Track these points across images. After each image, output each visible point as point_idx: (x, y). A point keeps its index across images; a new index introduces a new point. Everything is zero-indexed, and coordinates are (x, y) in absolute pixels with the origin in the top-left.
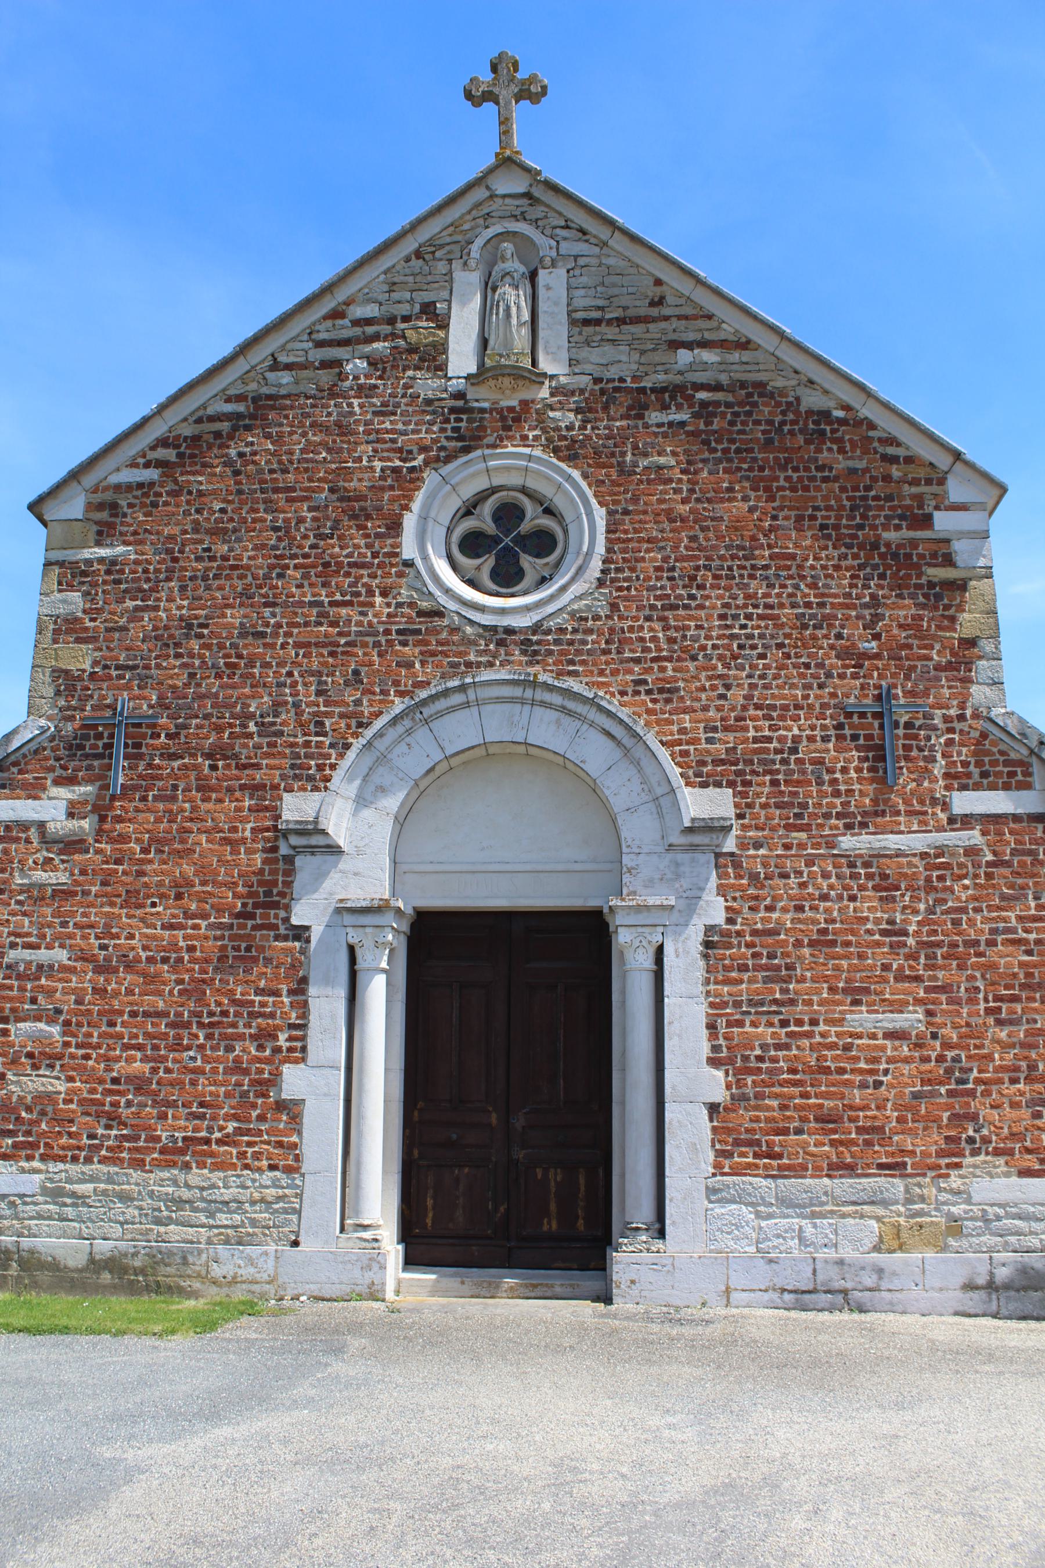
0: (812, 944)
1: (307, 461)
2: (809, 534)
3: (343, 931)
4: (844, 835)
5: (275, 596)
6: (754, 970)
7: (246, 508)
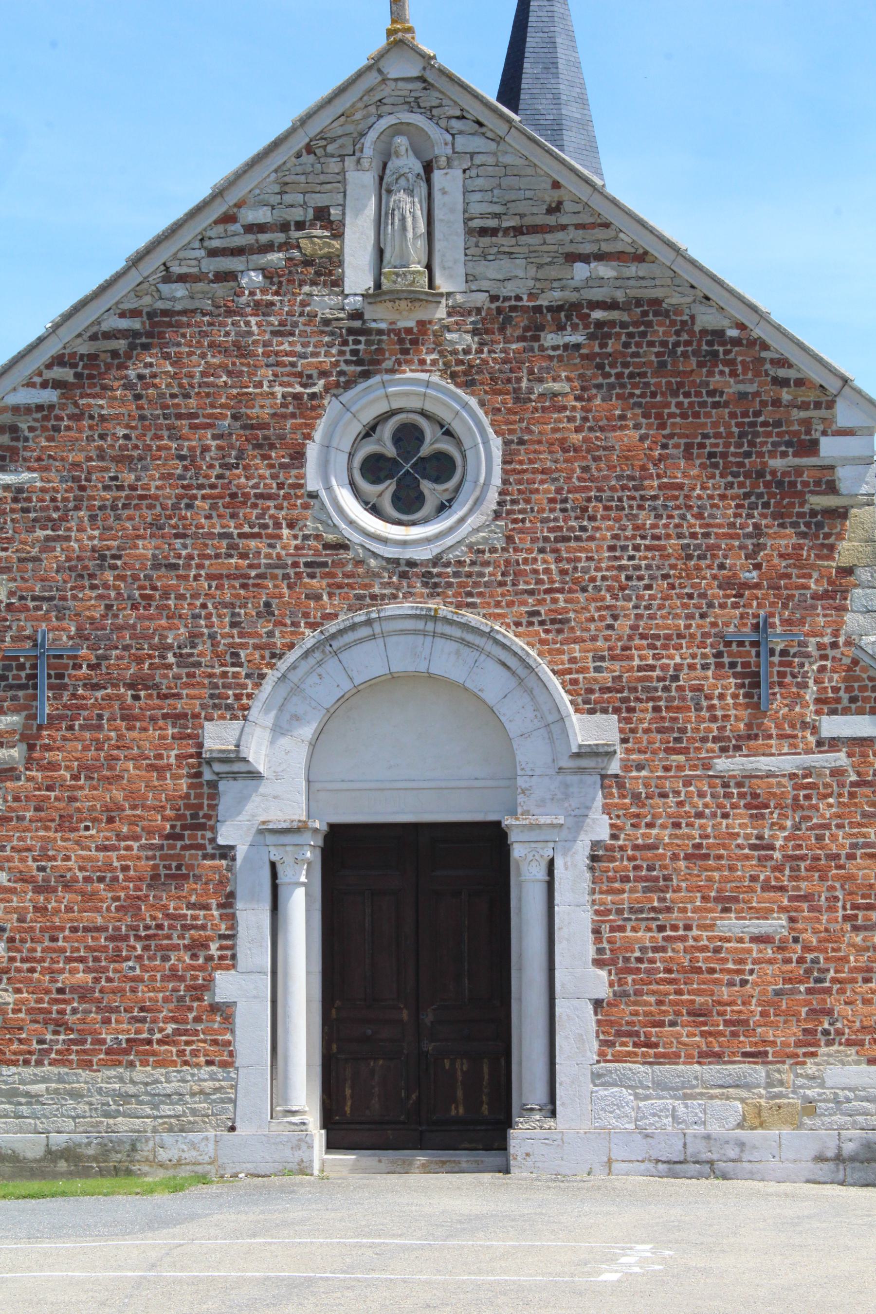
0: (687, 857)
1: (208, 385)
2: (698, 462)
4: (720, 757)
6: (635, 881)
7: (150, 435)
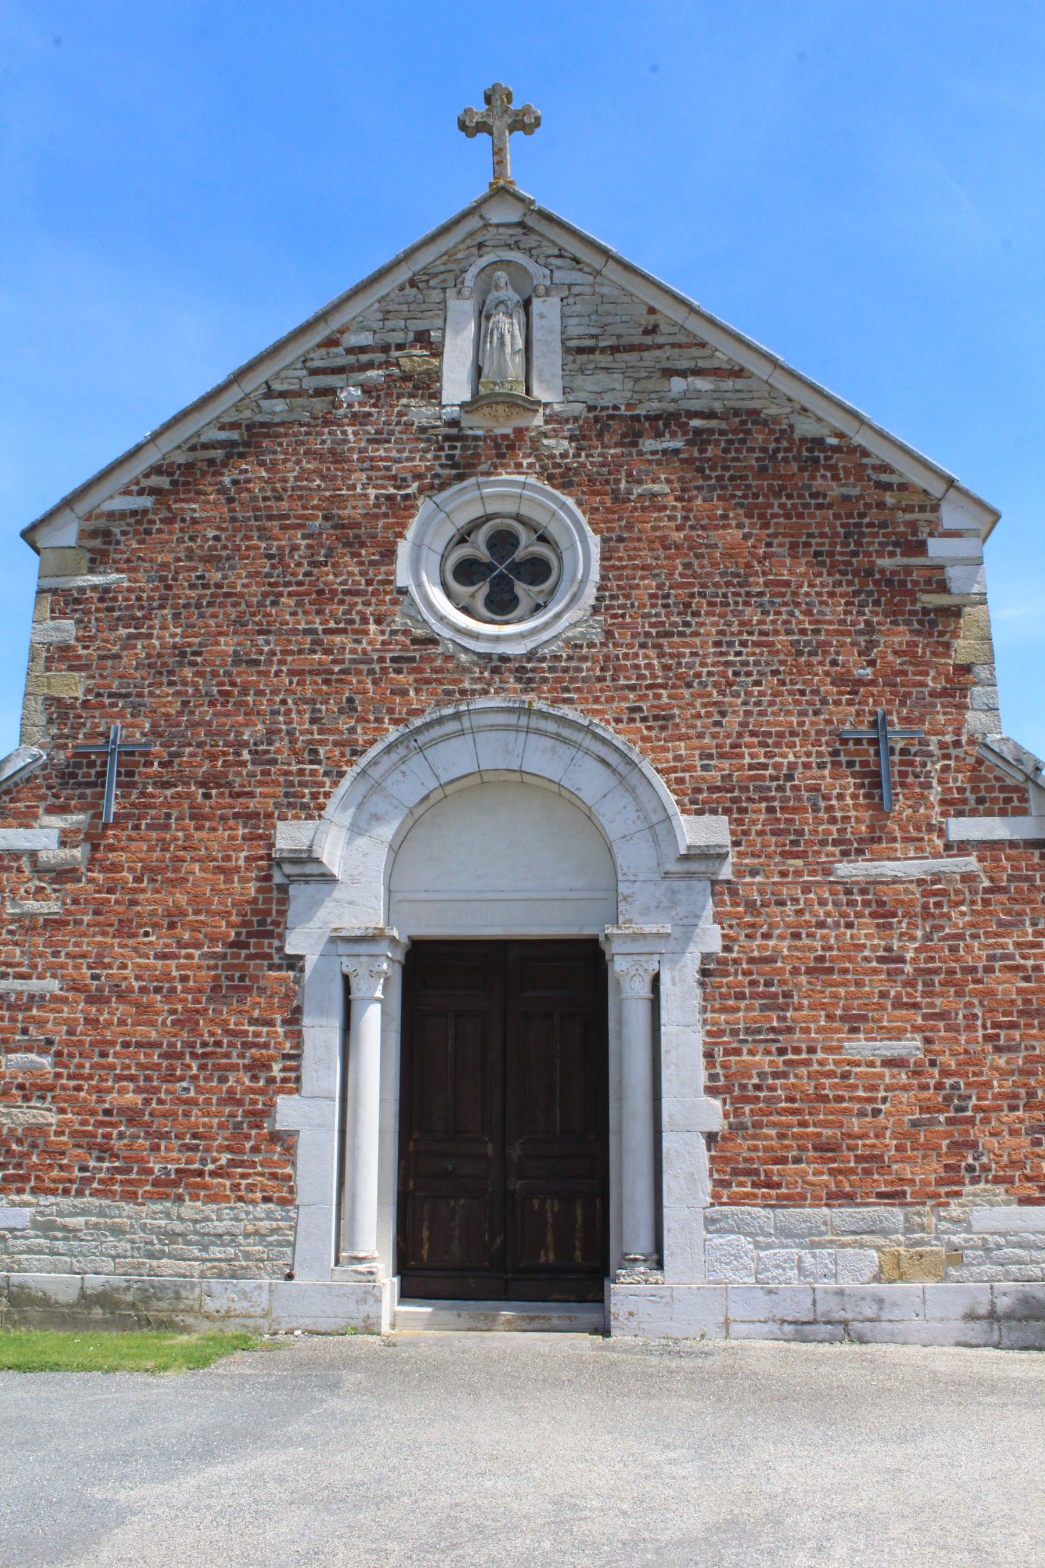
0: (809, 971)
1: (301, 488)
2: (804, 560)
3: (337, 960)
4: (841, 861)
5: (269, 623)
6: (751, 998)
7: (240, 535)
